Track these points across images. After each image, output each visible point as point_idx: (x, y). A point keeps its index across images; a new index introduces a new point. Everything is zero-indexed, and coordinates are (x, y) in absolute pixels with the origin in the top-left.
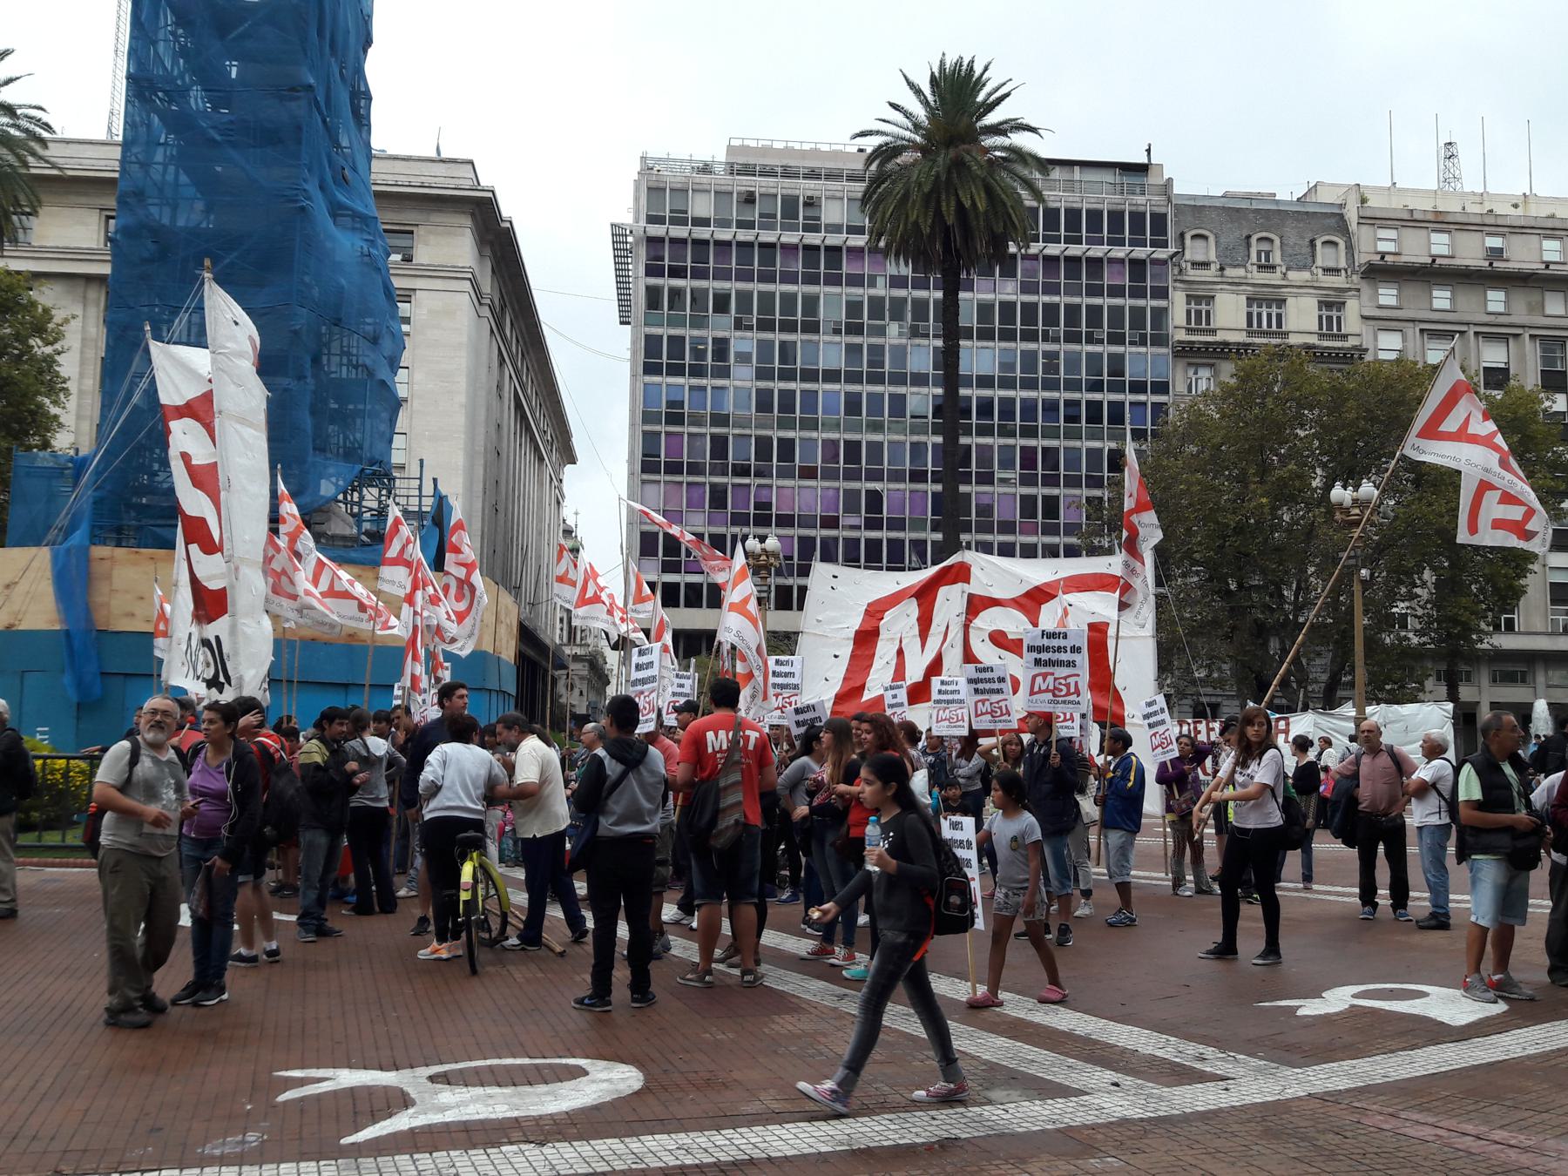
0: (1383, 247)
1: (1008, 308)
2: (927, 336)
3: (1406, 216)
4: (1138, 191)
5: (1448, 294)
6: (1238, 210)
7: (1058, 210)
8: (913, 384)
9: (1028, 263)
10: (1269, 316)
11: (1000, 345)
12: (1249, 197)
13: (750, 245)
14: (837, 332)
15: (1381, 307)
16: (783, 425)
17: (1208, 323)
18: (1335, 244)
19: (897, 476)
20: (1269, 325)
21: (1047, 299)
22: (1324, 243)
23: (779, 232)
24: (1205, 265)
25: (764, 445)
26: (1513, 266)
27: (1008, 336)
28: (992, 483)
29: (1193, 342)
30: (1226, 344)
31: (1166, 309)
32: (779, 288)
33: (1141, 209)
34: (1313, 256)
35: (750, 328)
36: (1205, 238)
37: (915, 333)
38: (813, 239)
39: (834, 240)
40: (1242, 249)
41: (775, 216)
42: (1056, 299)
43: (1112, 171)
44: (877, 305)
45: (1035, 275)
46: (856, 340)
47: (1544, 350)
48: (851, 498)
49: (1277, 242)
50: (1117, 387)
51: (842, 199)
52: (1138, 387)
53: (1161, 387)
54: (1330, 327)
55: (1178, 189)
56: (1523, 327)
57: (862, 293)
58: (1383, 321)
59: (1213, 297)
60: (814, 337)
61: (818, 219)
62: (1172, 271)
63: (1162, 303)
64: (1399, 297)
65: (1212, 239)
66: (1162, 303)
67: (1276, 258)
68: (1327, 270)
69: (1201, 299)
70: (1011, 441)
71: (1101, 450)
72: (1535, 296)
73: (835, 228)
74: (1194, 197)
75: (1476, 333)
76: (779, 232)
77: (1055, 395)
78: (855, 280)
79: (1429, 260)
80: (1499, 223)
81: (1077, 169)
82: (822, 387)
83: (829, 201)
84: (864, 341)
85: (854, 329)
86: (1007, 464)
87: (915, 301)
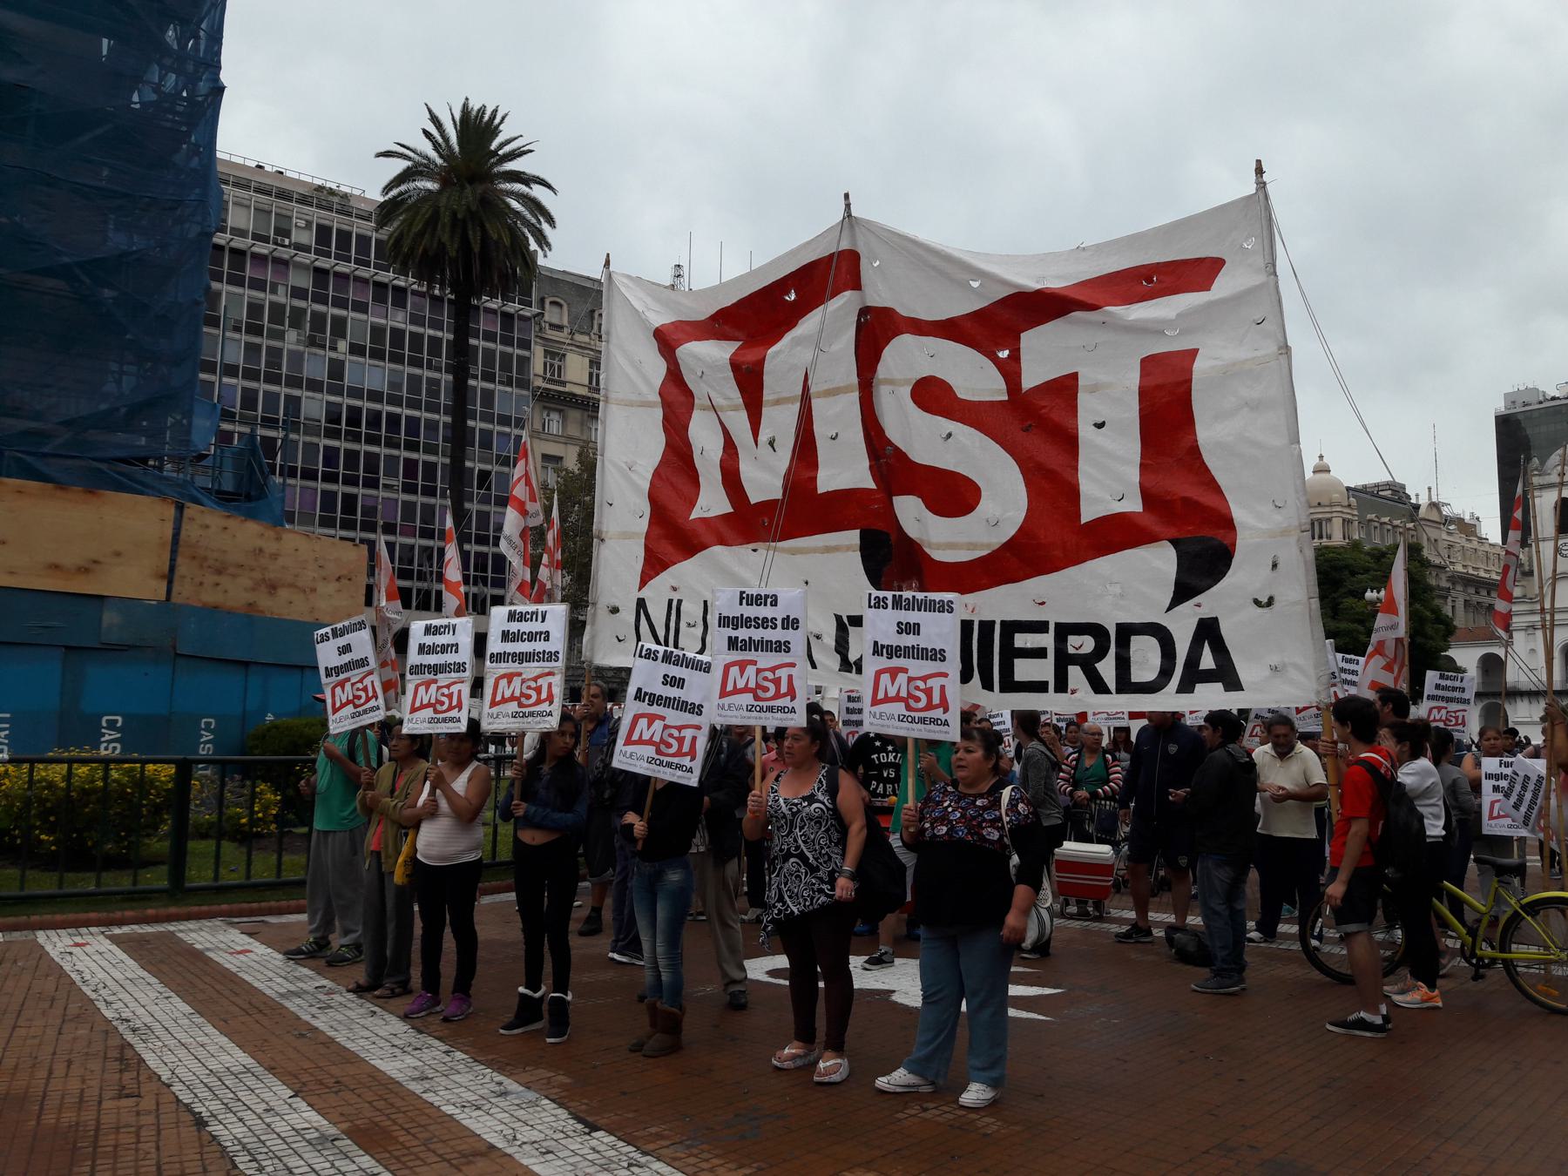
1: (397, 334)
2: (323, 347)
8: (308, 389)
9: (417, 299)
11: (388, 365)
14: (237, 329)
17: (559, 376)
21: (431, 332)
24: (559, 328)
27: (397, 358)
29: (550, 390)
30: (574, 395)
31: (529, 359)
36: (560, 306)
37: (312, 342)
39: (239, 243)
42: (439, 334)
44: (277, 310)
45: (422, 309)
46: (256, 340)
59: (564, 355)
62: (534, 328)
63: (526, 353)
66: (526, 353)
69: (555, 355)
77: (436, 417)
78: (258, 285)
83: (237, 208)
87: (314, 313)
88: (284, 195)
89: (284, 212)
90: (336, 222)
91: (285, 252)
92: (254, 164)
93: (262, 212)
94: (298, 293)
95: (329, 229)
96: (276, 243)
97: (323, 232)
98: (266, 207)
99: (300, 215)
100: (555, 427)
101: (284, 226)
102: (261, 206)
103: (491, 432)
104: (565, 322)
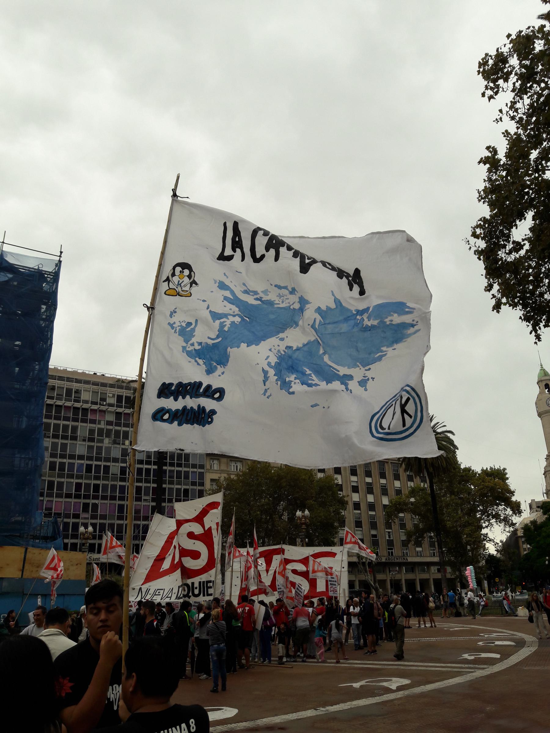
2: (119, 444)
13: (52, 405)
16: (60, 476)
19: (104, 498)
23: (64, 402)
25: (51, 484)
28: (141, 501)
32: (62, 422)
35: (49, 437)
37: (115, 442)
38: (77, 405)
39: (85, 406)
41: (62, 395)
44: (101, 431)
46: (92, 444)
48: (86, 507)
50: (187, 466)
51: (90, 391)
52: (194, 466)
53: (202, 467)
57: (96, 427)
60: (75, 442)
61: (80, 398)
70: (148, 485)
71: (181, 489)
73: (86, 402)
76: (64, 402)
78: (93, 422)
82: (77, 462)
83: (85, 392)
84: (95, 444)
85: (91, 440)
86: (147, 494)
88: (104, 385)
89: (104, 392)
90: (125, 393)
91: (104, 408)
92: (92, 373)
93: (95, 393)
94: (109, 423)
95: (122, 396)
96: (100, 404)
97: (120, 398)
98: (97, 391)
99: (110, 392)
100: (216, 467)
101: (103, 397)
102: (94, 390)
103: (188, 472)
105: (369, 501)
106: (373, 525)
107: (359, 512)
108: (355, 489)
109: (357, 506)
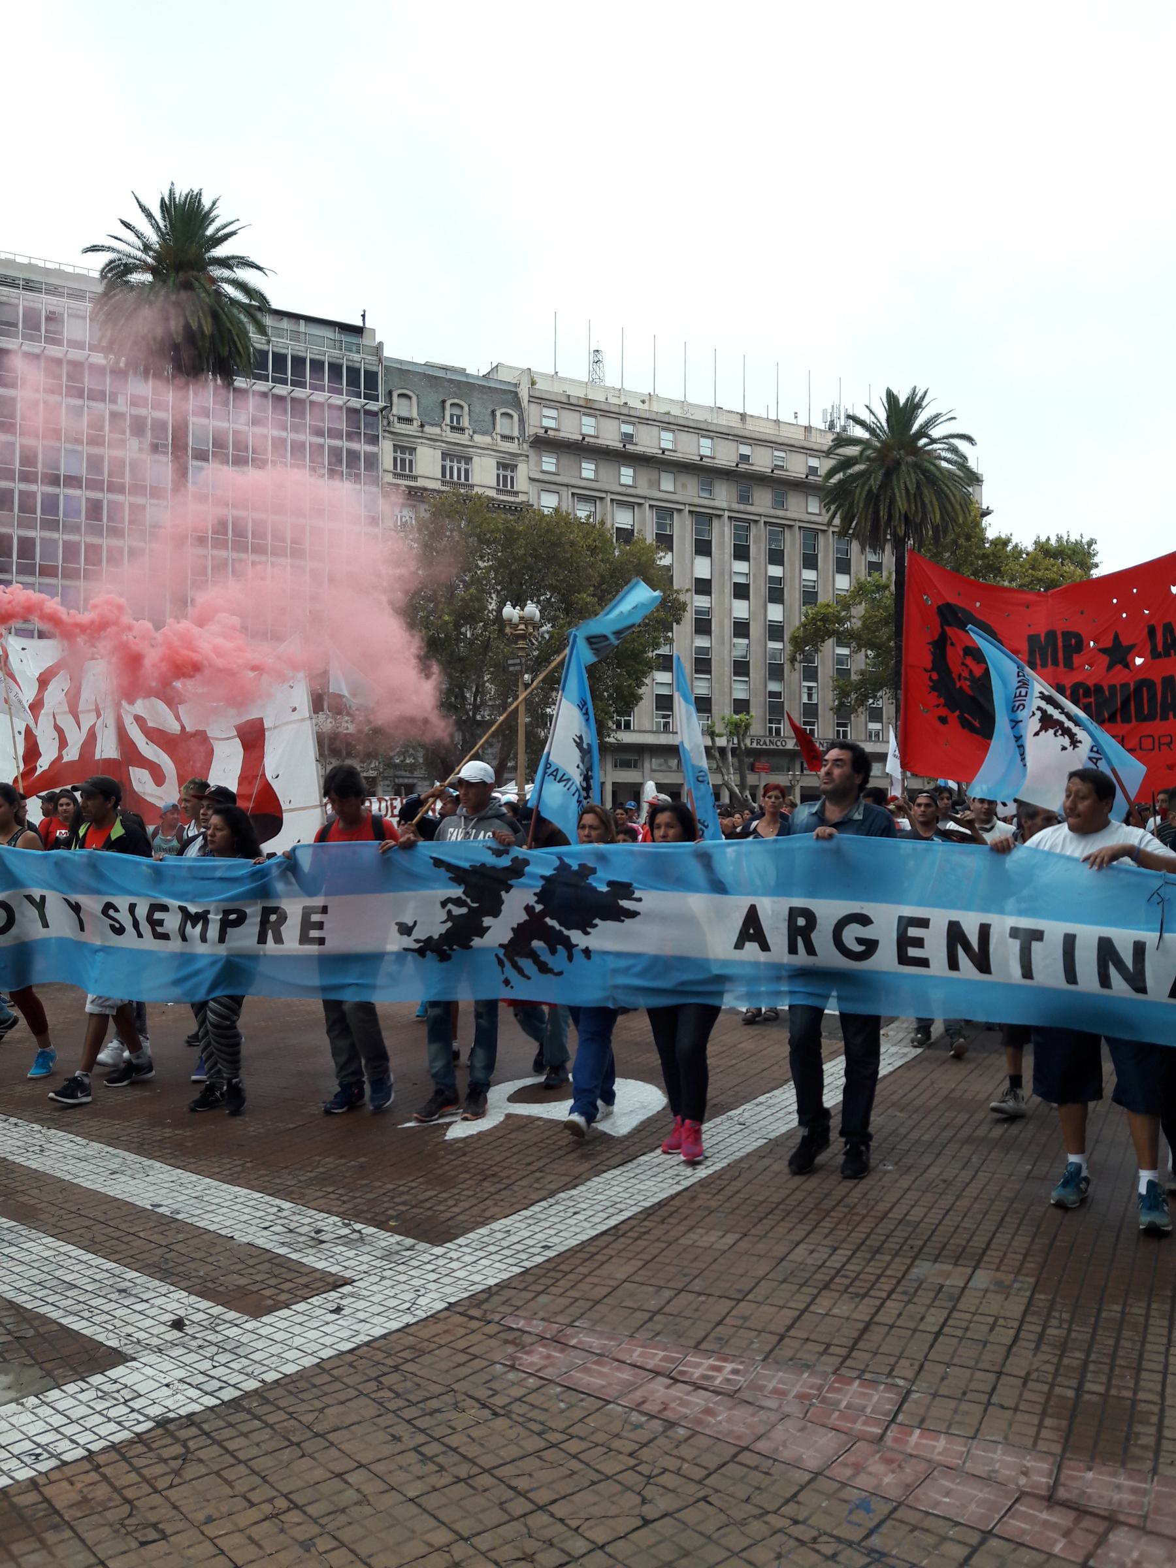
0: (547, 423)
3: (564, 400)
4: (354, 348)
5: (593, 467)
6: (436, 378)
7: (285, 356)
10: (459, 470)
12: (445, 369)
15: (543, 472)
17: (411, 470)
18: (511, 416)
20: (459, 477)
22: (503, 414)
24: (409, 421)
26: (639, 449)
33: (357, 365)
34: (494, 424)
36: (409, 397)
40: (439, 410)
43: (332, 329)
47: (658, 518)
49: (466, 408)
54: (505, 485)
55: (387, 353)
56: (645, 498)
58: (545, 484)
62: (382, 423)
64: (557, 465)
65: (414, 399)
67: (465, 422)
68: (504, 437)
69: (404, 450)
72: (654, 474)
74: (401, 362)
75: (612, 500)
79: (580, 438)
80: (632, 413)
81: (302, 322)
104: (415, 414)
105: (770, 617)
106: (775, 672)
107: (746, 641)
108: (741, 592)
109: (741, 629)
